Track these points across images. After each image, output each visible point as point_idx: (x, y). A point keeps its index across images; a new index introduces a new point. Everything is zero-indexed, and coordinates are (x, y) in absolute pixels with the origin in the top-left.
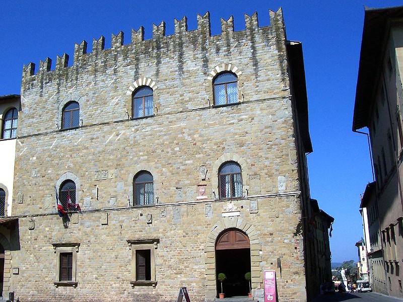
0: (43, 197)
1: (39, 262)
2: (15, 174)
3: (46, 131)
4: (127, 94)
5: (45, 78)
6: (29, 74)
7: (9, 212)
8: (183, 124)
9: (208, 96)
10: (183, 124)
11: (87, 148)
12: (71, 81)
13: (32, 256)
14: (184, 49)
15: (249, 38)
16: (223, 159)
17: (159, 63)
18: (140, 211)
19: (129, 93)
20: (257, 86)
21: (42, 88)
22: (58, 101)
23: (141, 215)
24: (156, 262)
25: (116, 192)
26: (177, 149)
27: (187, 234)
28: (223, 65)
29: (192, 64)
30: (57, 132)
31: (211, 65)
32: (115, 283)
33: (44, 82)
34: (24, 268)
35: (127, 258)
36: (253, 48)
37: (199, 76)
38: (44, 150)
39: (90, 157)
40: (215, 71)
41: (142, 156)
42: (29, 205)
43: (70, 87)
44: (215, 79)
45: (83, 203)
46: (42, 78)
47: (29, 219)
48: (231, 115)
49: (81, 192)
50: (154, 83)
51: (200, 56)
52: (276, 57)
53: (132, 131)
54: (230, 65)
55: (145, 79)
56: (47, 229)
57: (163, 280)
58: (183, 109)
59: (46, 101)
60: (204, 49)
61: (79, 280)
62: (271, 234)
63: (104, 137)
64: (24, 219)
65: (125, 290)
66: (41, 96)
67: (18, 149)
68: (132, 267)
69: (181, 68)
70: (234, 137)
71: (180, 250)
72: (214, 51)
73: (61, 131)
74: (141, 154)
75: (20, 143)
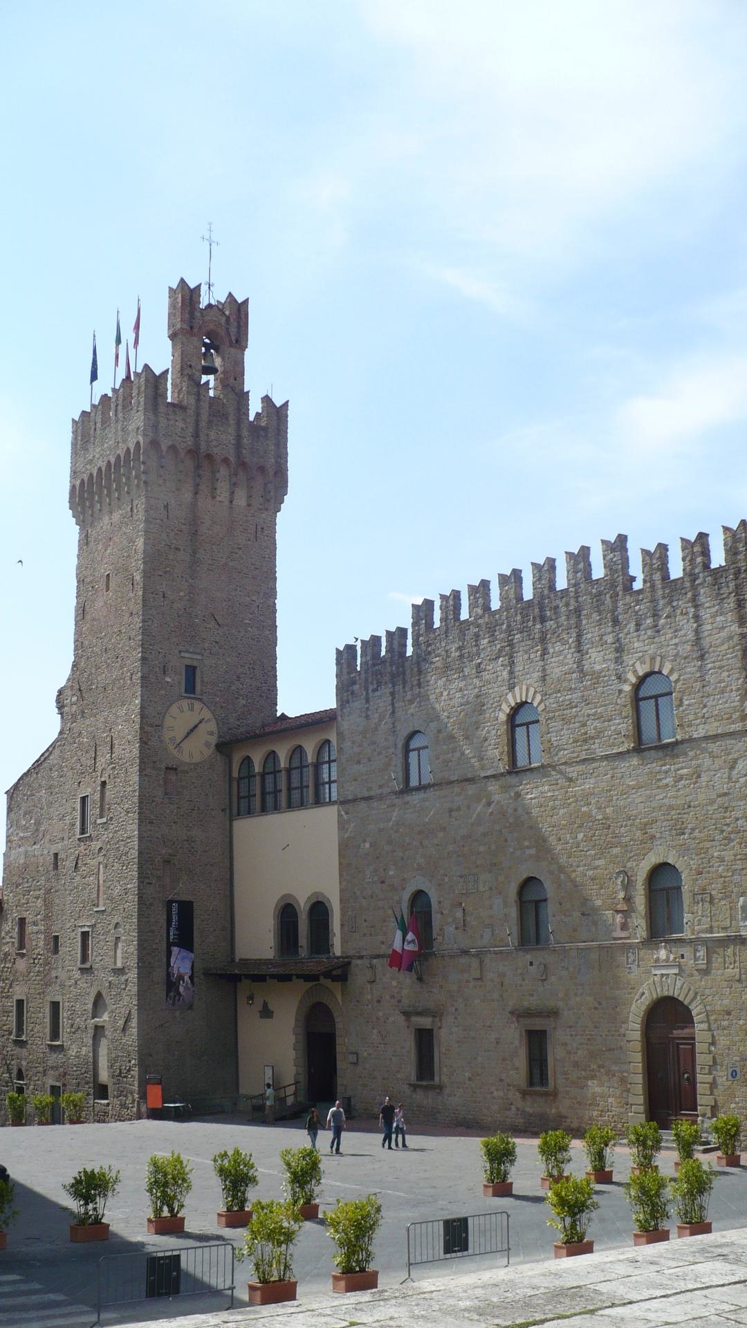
0: (385, 921)
1: (385, 1044)
2: (341, 875)
3: (379, 791)
4: (500, 721)
5: (370, 680)
6: (345, 671)
7: (337, 950)
8: (589, 785)
9: (626, 726)
10: (589, 785)
11: (444, 829)
12: (411, 689)
13: (375, 1031)
14: (584, 622)
15: (689, 595)
16: (652, 859)
17: (545, 652)
18: (529, 957)
19: (502, 717)
20: (705, 706)
21: (367, 701)
22: (393, 731)
23: (531, 964)
24: (555, 1054)
25: (491, 917)
26: (580, 836)
27: (600, 1003)
28: (648, 660)
29: (597, 659)
30: (395, 793)
31: (629, 660)
32: (497, 1090)
33: (371, 688)
34: (365, 1054)
35: (512, 1043)
36: (697, 617)
37: (610, 683)
38: (380, 830)
39: (451, 848)
40: (635, 672)
41: (528, 847)
42: (364, 935)
43: (411, 702)
44: (637, 687)
45: (443, 937)
46: (366, 680)
47: (366, 962)
48: (664, 768)
49: (439, 915)
50: (538, 698)
51: (610, 639)
52: (736, 639)
53: (511, 797)
54: (658, 659)
55: (524, 687)
56: (394, 983)
57: (568, 1089)
58: (586, 755)
59: (376, 729)
60: (616, 622)
61: (445, 1079)
62: (729, 1013)
63: (469, 807)
64: (359, 962)
65: (512, 1104)
66: (367, 717)
67: (342, 826)
68: (521, 1061)
69: (579, 663)
70: (668, 815)
71: (591, 1035)
72: (632, 626)
73: (402, 792)
74: (526, 843)
75: (343, 813)
